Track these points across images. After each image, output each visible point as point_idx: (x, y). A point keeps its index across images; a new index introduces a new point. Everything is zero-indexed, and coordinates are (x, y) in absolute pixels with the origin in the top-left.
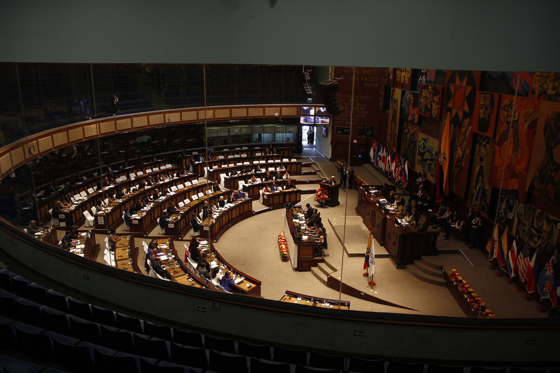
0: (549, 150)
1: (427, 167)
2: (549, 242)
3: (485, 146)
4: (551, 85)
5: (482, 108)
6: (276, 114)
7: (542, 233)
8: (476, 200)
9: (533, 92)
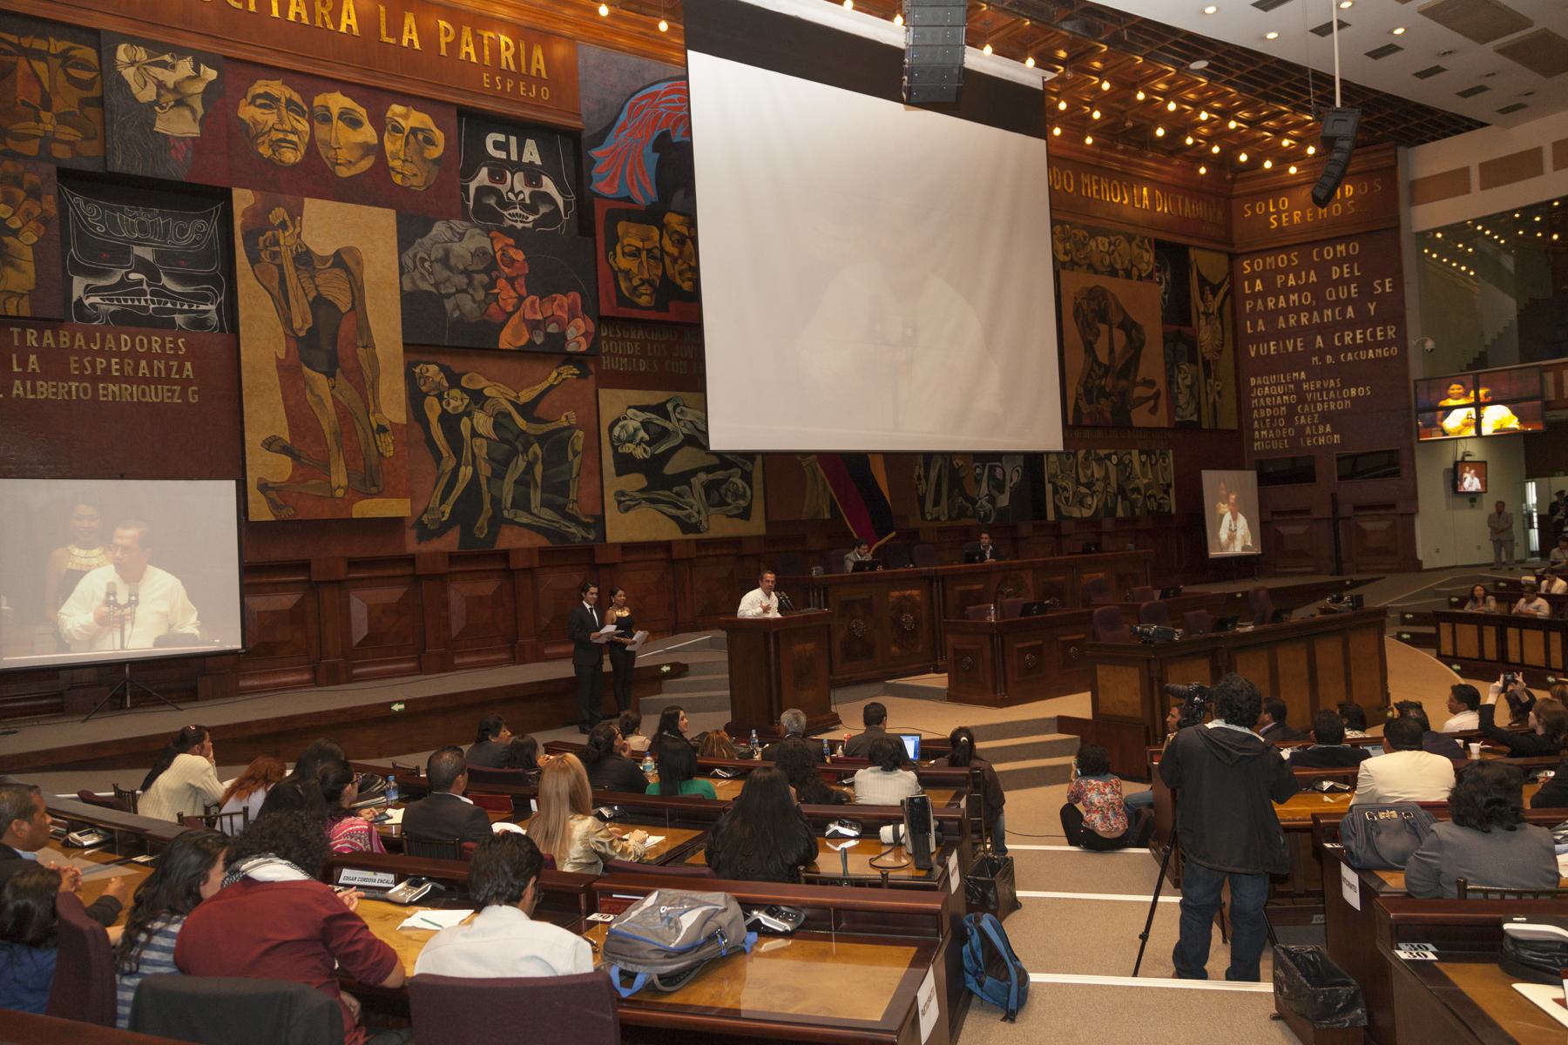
0: (1089, 347)
1: (695, 502)
8: (937, 503)
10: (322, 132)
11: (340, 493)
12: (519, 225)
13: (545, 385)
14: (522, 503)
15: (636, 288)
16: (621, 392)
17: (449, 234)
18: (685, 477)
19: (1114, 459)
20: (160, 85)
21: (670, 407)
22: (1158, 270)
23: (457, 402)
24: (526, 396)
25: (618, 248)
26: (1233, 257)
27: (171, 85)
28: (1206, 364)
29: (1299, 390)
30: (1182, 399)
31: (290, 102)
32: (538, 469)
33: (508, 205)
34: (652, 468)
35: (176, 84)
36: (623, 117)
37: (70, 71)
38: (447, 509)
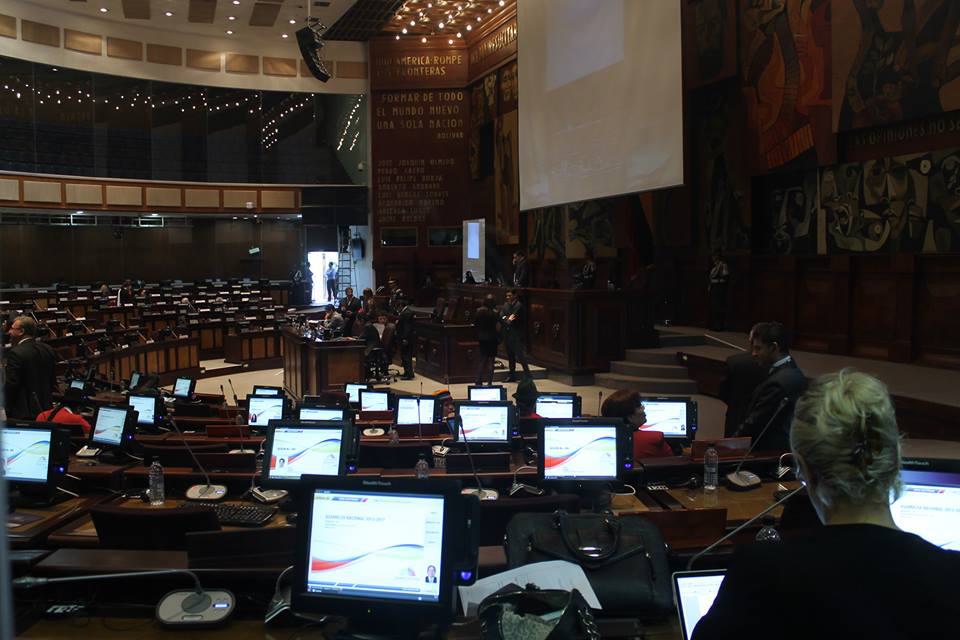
2: (909, 215)
6: (249, 205)
7: (887, 206)
19: (926, 166)
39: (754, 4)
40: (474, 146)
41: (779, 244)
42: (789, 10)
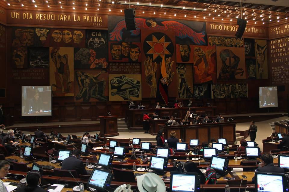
1: (127, 94)
3: (182, 69)
4: (217, 41)
5: (183, 51)
8: (183, 94)
9: (210, 44)
10: (64, 36)
11: (63, 92)
12: (97, 47)
13: (99, 74)
14: (94, 94)
15: (116, 57)
16: (113, 75)
17: (83, 50)
18: (125, 90)
19: (231, 86)
20: (41, 33)
21: (122, 77)
22: (246, 44)
23: (83, 77)
24: (95, 76)
25: (113, 50)
26: (268, 41)
27: (42, 33)
28: (259, 65)
29: (282, 71)
30: (251, 73)
31: (59, 33)
32: (97, 89)
33: (96, 44)
34: (119, 88)
35: (43, 33)
36: (116, 26)
37: (31, 34)
38: (81, 95)
39: (197, 51)
40: (19, 53)
41: (196, 97)
42: (206, 55)
